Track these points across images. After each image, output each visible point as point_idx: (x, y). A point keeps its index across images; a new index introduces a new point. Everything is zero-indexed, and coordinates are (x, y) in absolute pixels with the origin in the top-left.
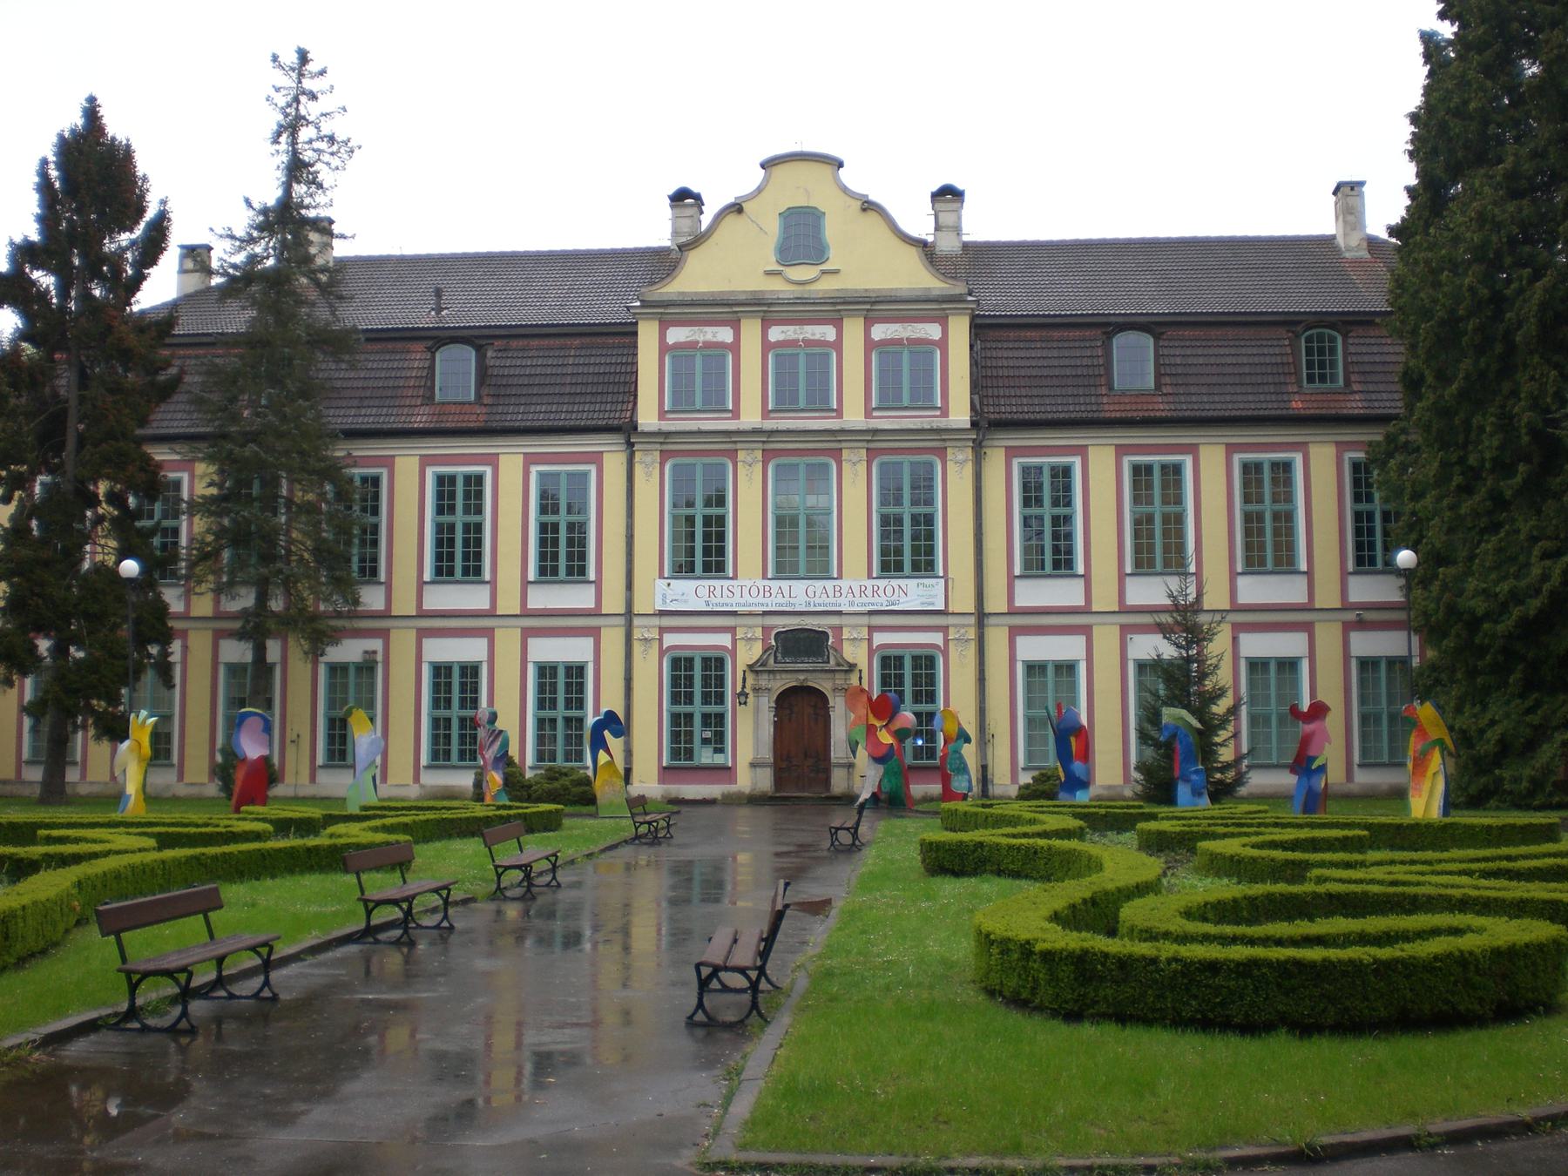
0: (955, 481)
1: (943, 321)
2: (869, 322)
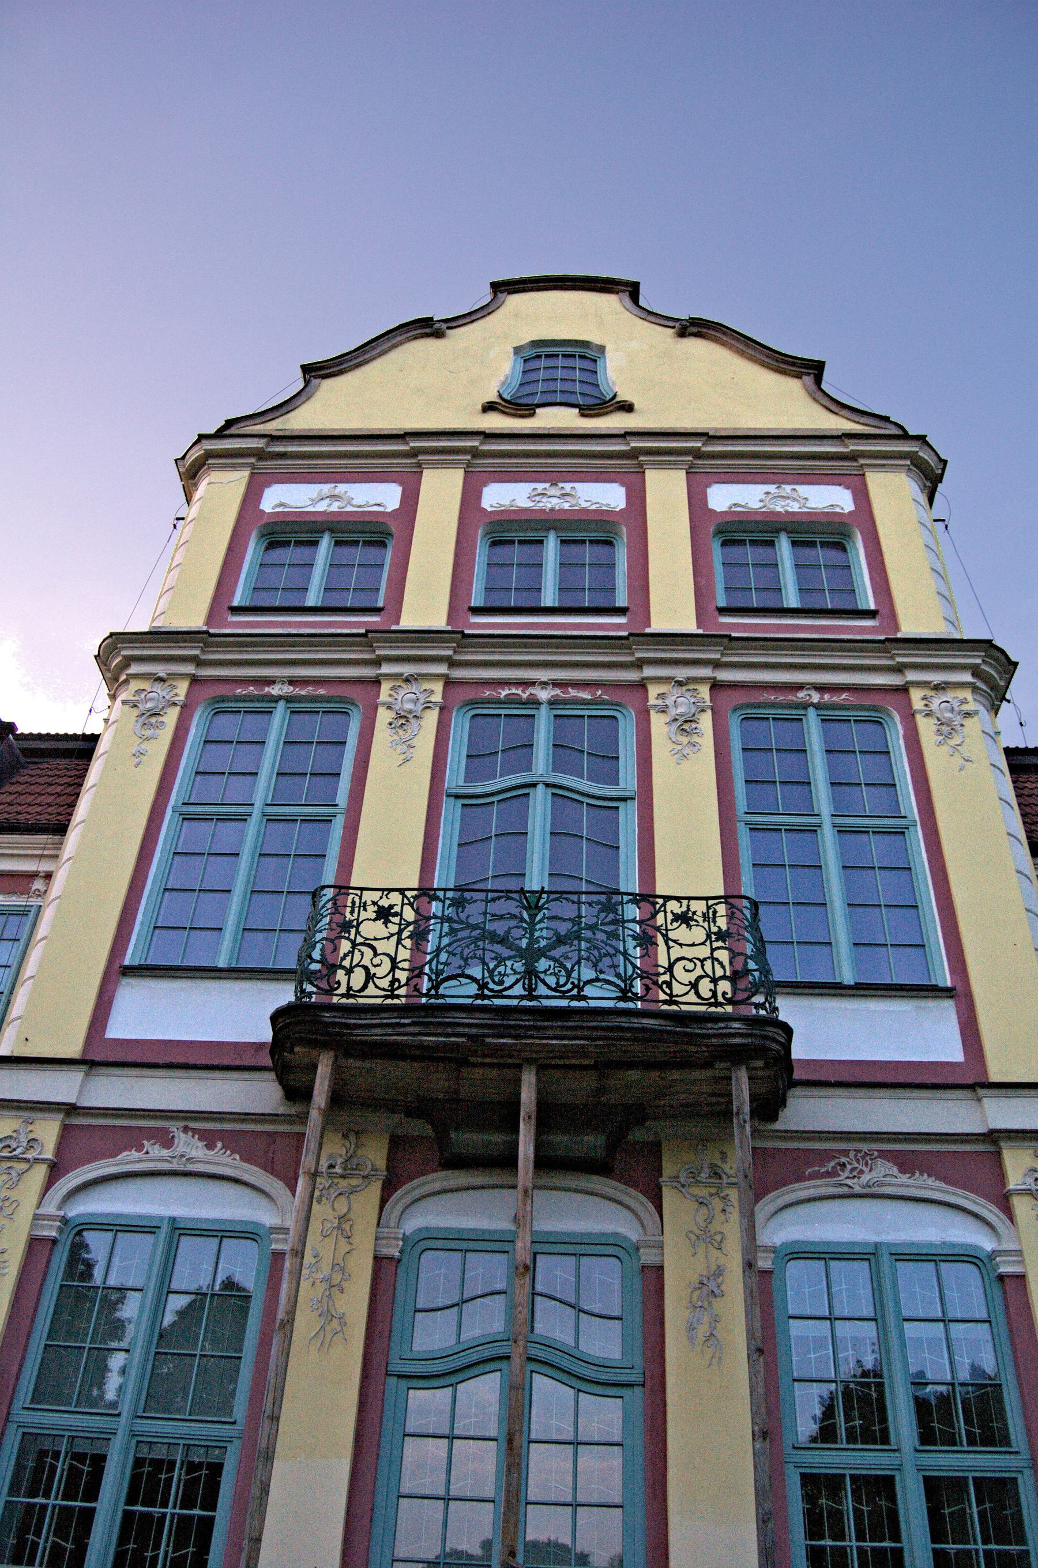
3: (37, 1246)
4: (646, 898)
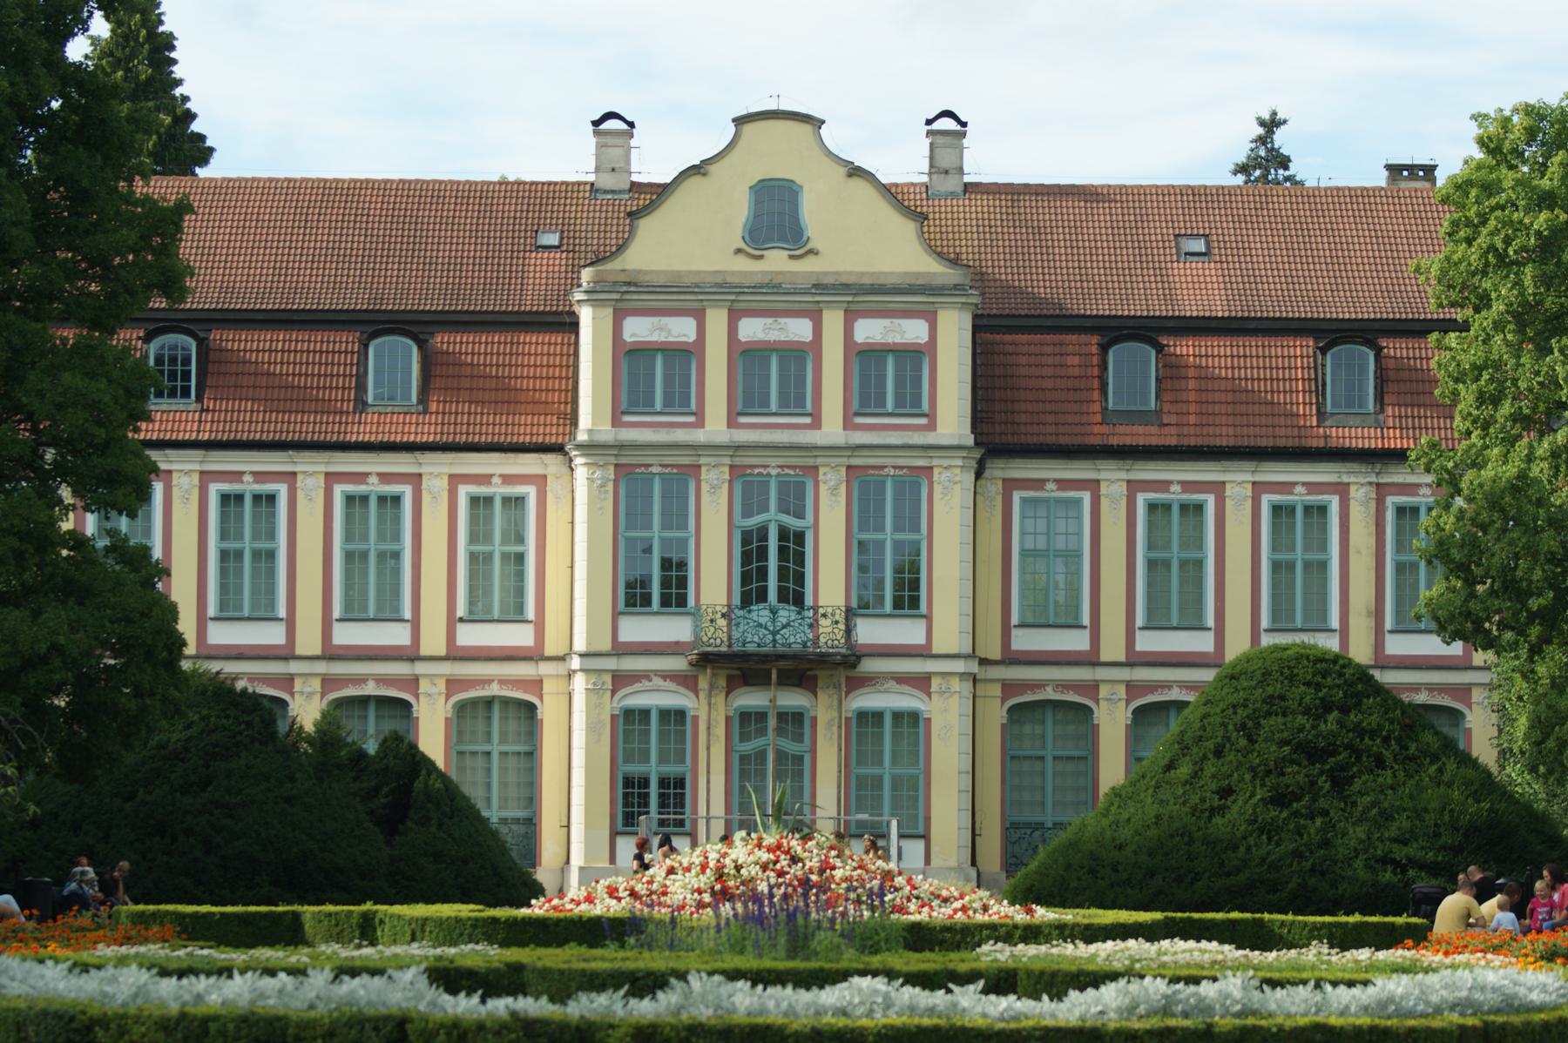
0: (950, 503)
1: (931, 319)
2: (851, 316)
3: (613, 717)
4: (815, 608)
